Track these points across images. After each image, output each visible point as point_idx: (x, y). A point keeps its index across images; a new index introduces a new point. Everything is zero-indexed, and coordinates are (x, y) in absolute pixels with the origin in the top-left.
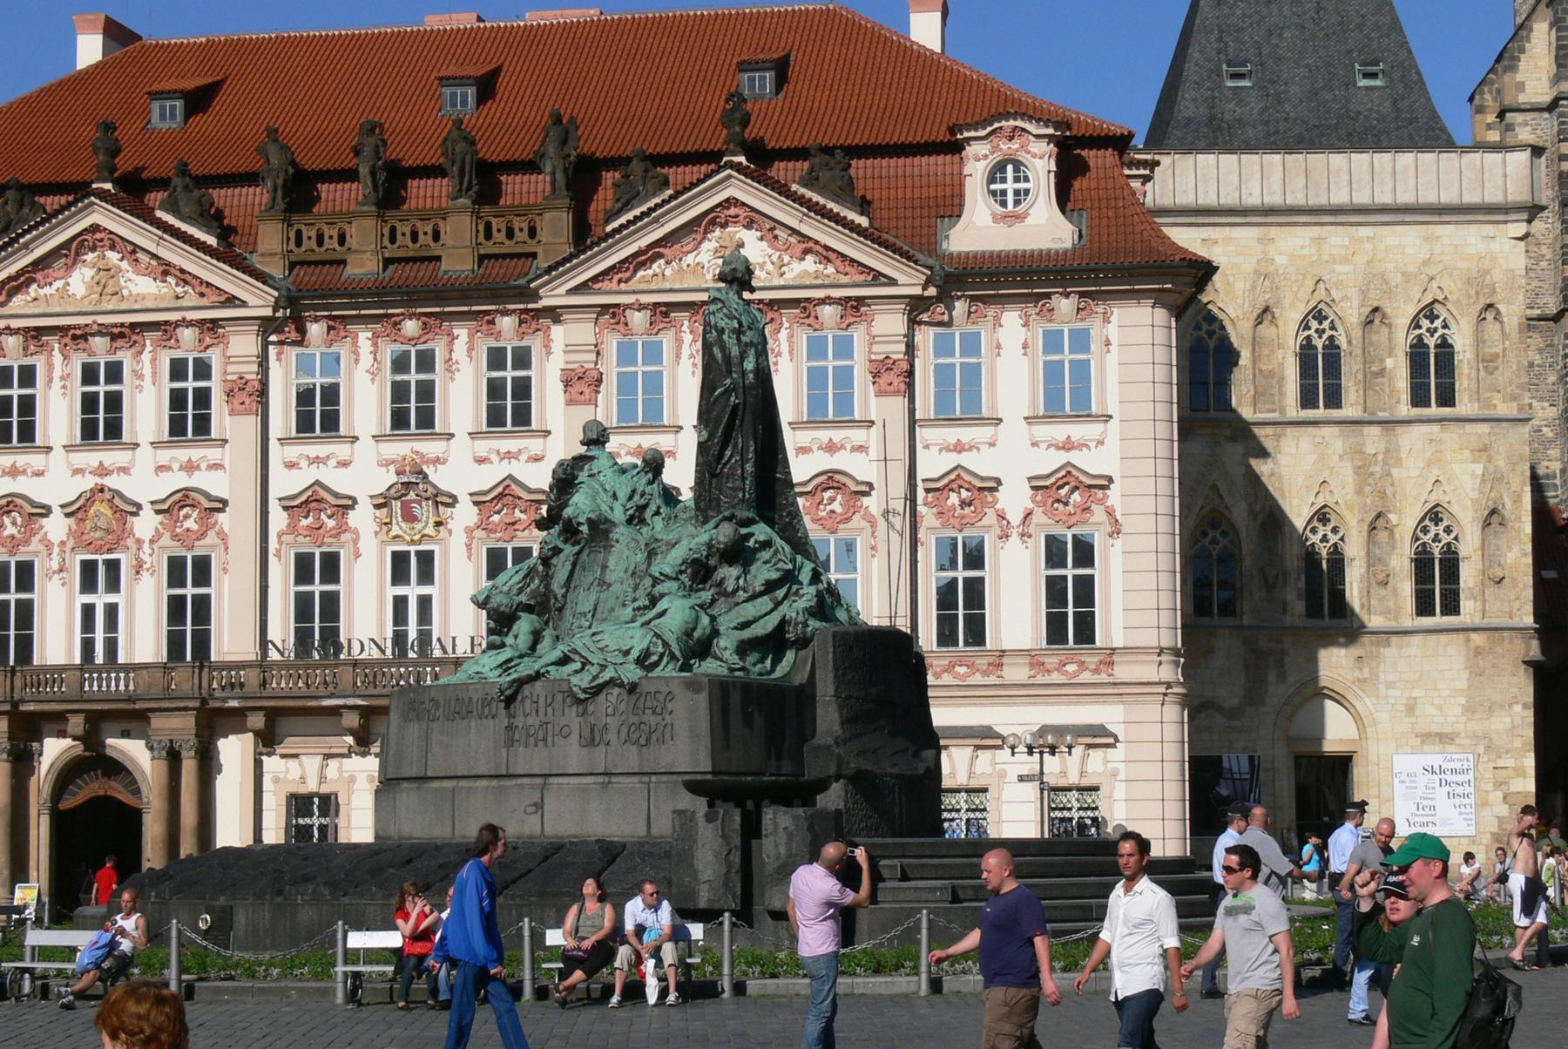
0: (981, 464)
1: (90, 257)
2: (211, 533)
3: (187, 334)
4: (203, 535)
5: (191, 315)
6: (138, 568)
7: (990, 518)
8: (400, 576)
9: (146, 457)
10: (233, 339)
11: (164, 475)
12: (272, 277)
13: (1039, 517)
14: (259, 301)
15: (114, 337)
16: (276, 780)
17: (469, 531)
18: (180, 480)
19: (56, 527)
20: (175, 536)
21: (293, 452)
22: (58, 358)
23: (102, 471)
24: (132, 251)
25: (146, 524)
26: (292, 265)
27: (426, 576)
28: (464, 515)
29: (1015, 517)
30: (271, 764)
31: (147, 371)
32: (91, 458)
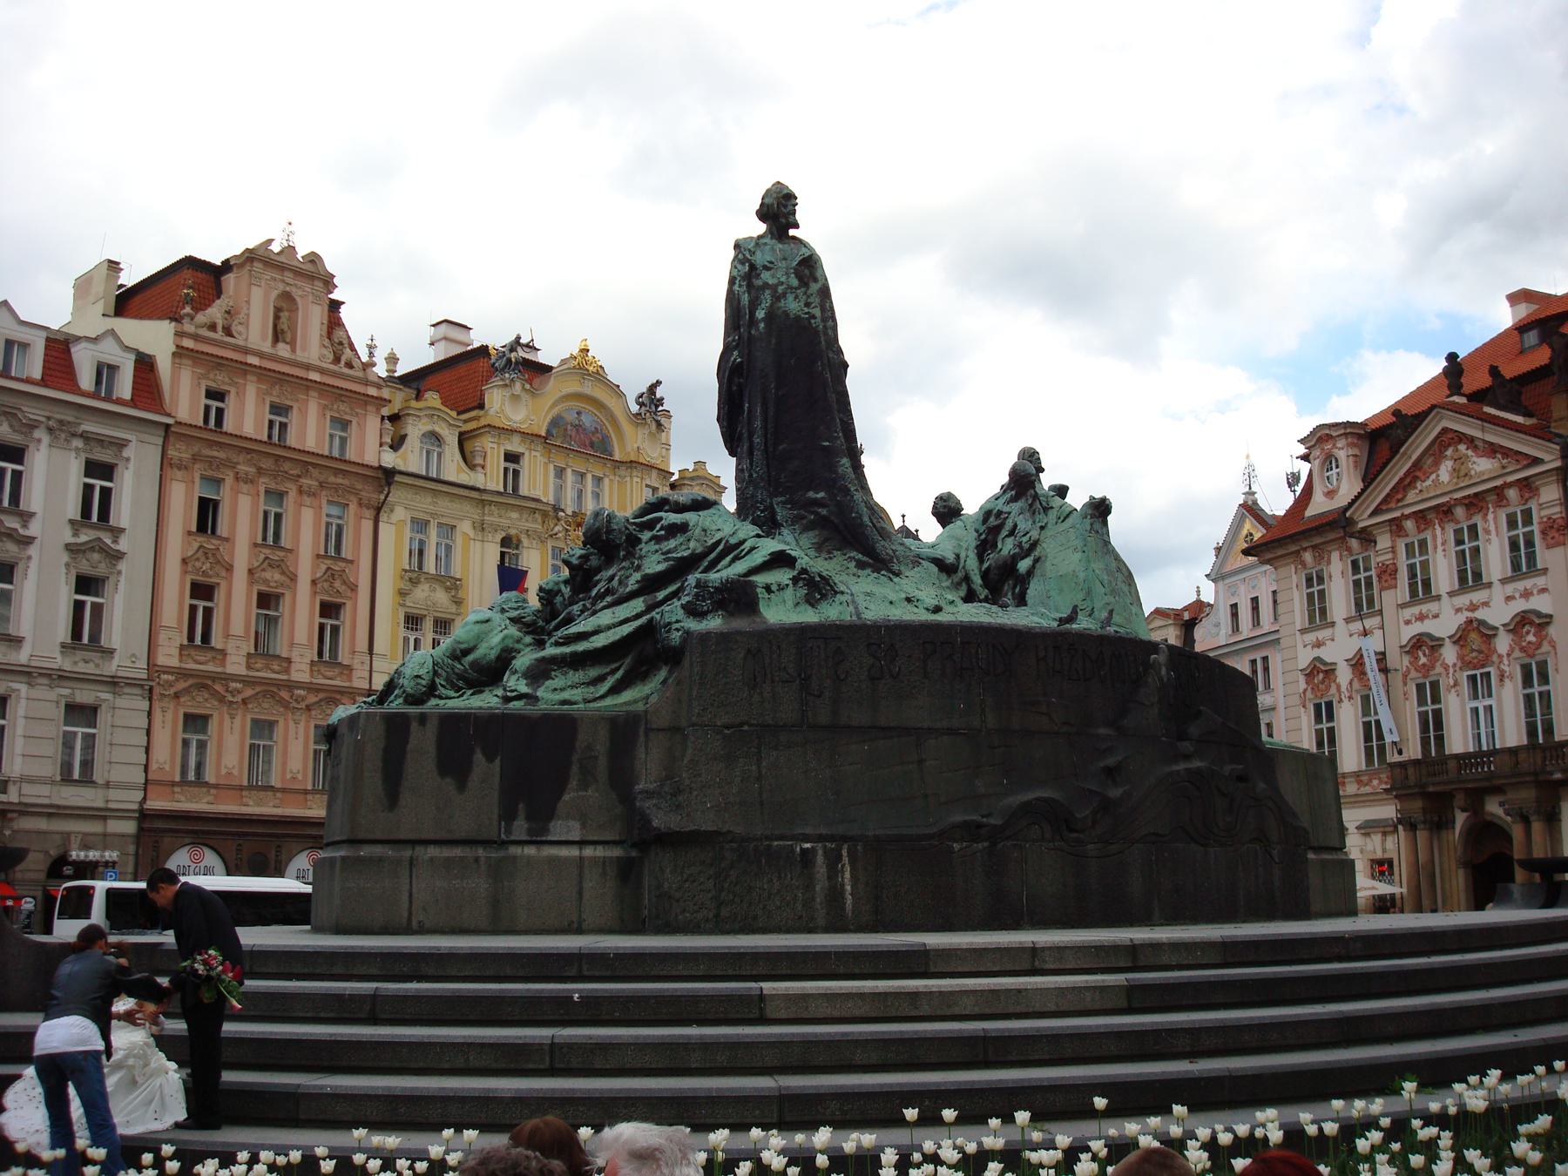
1: (1449, 452)
2: (1545, 643)
4: (1539, 646)
5: (1510, 479)
6: (1502, 678)
9: (1498, 592)
10: (1542, 490)
11: (1513, 603)
12: (1560, 436)
18: (1520, 605)
19: (1449, 654)
20: (1522, 649)
22: (1438, 531)
23: (1473, 607)
24: (1471, 441)
25: (1503, 643)
31: (1492, 528)
32: (1463, 600)
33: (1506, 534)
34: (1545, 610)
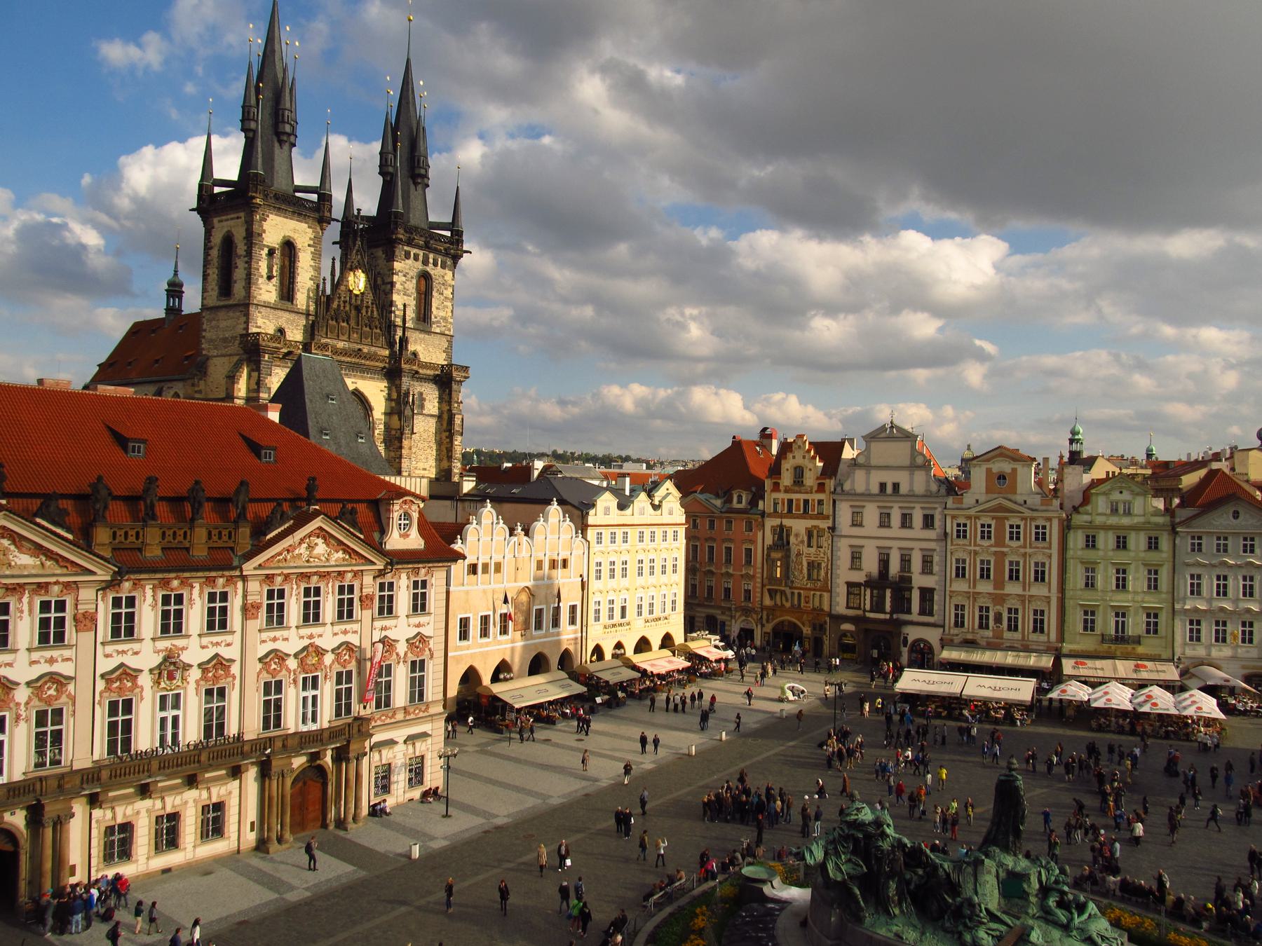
0: (391, 634)
3: (56, 588)
6: (18, 718)
7: (394, 656)
8: (163, 708)
11: (34, 666)
13: (409, 655)
14: (103, 575)
15: (7, 589)
16: (97, 821)
17: (197, 682)
18: (45, 668)
20: (40, 699)
21: (110, 649)
26: (114, 549)
27: (176, 706)
28: (195, 674)
29: (402, 655)
30: (97, 813)
31: (26, 608)
33: (38, 616)
34: (66, 673)
